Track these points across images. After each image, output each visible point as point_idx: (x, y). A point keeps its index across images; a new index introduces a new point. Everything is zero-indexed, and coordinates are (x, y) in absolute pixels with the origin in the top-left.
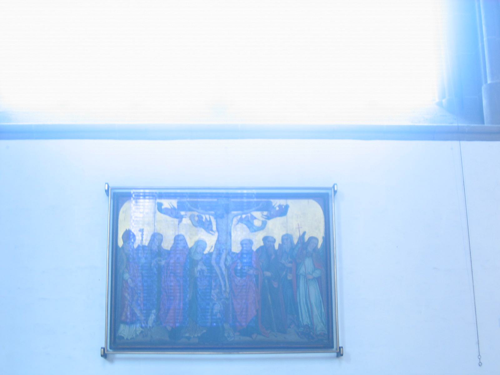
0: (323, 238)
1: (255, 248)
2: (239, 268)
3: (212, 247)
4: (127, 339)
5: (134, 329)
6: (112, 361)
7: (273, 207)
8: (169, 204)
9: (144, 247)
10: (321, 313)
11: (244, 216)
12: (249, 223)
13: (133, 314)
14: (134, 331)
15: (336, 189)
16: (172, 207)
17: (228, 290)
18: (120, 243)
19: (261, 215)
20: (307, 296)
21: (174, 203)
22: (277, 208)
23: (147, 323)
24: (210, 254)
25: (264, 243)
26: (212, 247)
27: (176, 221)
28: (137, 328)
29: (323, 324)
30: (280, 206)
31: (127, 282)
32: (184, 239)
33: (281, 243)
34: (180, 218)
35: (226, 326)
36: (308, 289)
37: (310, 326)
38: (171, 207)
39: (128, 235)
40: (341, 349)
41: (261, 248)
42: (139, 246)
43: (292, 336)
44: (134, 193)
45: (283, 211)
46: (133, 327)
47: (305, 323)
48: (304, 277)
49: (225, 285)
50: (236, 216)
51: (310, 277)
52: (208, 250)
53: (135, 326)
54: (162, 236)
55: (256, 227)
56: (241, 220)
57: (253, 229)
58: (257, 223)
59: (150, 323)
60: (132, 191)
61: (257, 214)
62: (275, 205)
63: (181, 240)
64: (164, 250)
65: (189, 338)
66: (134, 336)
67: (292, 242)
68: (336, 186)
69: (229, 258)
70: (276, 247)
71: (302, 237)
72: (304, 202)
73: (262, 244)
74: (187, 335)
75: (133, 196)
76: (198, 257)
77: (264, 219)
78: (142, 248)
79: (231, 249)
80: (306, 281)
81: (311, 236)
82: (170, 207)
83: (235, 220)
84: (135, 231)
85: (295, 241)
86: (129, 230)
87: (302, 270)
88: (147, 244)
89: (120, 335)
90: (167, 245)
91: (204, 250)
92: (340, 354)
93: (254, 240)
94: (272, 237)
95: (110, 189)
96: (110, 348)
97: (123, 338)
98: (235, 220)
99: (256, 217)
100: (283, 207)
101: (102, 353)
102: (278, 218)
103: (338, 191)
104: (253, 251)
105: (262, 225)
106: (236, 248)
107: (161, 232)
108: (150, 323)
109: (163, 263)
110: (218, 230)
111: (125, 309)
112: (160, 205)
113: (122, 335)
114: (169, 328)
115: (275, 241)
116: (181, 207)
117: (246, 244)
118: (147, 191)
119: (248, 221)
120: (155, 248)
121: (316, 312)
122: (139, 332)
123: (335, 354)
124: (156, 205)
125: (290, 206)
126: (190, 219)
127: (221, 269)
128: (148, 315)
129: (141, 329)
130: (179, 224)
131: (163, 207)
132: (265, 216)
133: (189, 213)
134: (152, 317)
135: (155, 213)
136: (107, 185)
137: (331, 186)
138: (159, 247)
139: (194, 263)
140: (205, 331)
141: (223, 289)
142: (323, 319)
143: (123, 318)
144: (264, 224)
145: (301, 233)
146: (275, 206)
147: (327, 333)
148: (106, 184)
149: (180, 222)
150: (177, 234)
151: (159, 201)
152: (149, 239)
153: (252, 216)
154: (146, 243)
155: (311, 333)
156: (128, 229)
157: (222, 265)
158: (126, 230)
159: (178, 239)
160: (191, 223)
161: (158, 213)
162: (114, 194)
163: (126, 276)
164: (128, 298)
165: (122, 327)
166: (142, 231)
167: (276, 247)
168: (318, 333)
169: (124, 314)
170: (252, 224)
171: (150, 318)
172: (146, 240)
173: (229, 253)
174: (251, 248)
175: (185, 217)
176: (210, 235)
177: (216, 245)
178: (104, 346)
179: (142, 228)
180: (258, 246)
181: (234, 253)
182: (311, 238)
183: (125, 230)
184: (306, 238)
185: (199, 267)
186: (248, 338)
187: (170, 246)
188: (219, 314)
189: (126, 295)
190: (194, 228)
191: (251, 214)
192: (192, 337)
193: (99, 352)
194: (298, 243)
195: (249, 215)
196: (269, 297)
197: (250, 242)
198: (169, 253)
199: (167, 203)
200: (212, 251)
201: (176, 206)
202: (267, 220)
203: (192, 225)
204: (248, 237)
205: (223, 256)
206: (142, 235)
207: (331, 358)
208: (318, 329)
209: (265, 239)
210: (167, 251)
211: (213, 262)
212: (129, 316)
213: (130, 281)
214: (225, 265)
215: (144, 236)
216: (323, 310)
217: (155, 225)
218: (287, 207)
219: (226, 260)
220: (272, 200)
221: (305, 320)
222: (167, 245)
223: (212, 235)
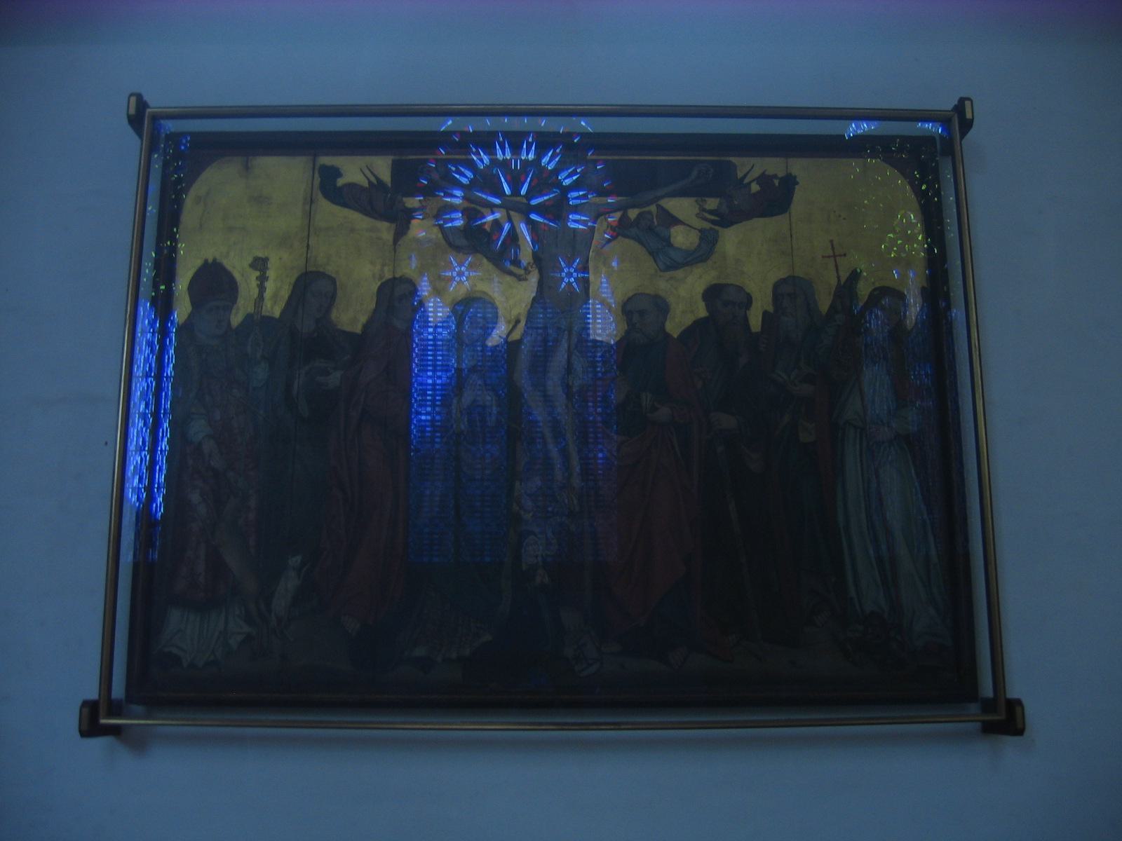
0: (923, 289)
1: (674, 327)
3: (518, 322)
8: (361, 170)
9: (268, 320)
11: (633, 214)
15: (969, 116)
16: (375, 182)
17: (576, 482)
19: (697, 210)
21: (382, 167)
22: (755, 188)
24: (511, 347)
25: (707, 306)
26: (518, 322)
27: (385, 230)
30: (764, 179)
32: (414, 291)
33: (771, 309)
34: (402, 220)
38: (370, 182)
40: (1018, 709)
41: (699, 325)
42: (249, 317)
54: (333, 281)
55: (679, 249)
56: (621, 229)
58: (682, 238)
61: (682, 207)
62: (745, 176)
64: (344, 332)
68: (967, 103)
69: (578, 364)
70: (755, 322)
71: (847, 288)
73: (702, 312)
74: (420, 652)
77: (707, 225)
78: (256, 322)
79: (585, 328)
82: (366, 184)
84: (238, 265)
85: (824, 304)
86: (215, 260)
88: (277, 313)
93: (671, 300)
94: (740, 289)
99: (681, 217)
100: (776, 182)
102: (758, 222)
103: (975, 123)
104: (667, 336)
105: (699, 245)
107: (330, 270)
109: (335, 379)
110: (537, 259)
112: (329, 175)
113: (175, 651)
115: (749, 300)
116: (406, 178)
117: (642, 313)
119: (650, 229)
123: (978, 725)
124: (317, 175)
125: (798, 180)
127: (546, 398)
130: (395, 241)
132: (711, 212)
134: (289, 584)
135: (312, 201)
136: (133, 100)
137: (948, 104)
140: (487, 638)
141: (559, 475)
145: (844, 275)
146: (746, 181)
149: (401, 231)
150: (388, 276)
151: (326, 160)
152: (285, 293)
153: (664, 213)
154: (274, 308)
156: (210, 261)
157: (554, 384)
158: (206, 261)
160: (440, 235)
165: (175, 615)
166: (260, 264)
167: (755, 322)
170: (667, 242)
172: (275, 296)
173: (584, 344)
176: (508, 278)
177: (530, 316)
178: (93, 693)
180: (688, 320)
182: (882, 292)
183: (199, 263)
184: (864, 290)
187: (363, 319)
189: (195, 497)
191: (660, 208)
193: (71, 720)
194: (832, 307)
195: (653, 208)
197: (661, 307)
198: (359, 342)
199: (353, 170)
200: (516, 335)
201: (386, 176)
203: (443, 242)
205: (560, 358)
209: (713, 294)
210: (349, 335)
211: (523, 378)
214: (567, 388)
215: (270, 286)
217: (308, 246)
218: (789, 183)
219: (569, 369)
220: (734, 160)
223: (520, 278)
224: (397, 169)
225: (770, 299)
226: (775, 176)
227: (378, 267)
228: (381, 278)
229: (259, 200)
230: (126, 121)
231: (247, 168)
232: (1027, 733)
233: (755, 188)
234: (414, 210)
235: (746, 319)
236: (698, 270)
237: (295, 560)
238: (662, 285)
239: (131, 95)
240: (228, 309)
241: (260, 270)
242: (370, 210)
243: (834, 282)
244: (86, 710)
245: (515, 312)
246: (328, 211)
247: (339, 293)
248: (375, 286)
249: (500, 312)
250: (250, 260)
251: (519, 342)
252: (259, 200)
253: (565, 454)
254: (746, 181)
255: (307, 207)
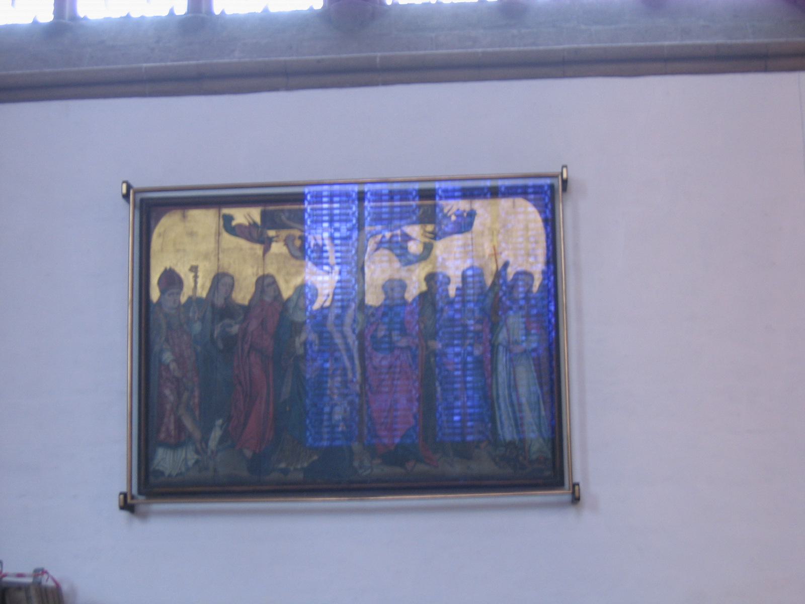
2: (381, 333)
4: (170, 476)
5: (184, 456)
6: (144, 516)
7: (446, 217)
8: (245, 217)
9: (199, 301)
10: (539, 416)
12: (398, 247)
13: (180, 427)
14: (183, 460)
15: (565, 176)
16: (251, 221)
18: (155, 294)
19: (422, 232)
20: (513, 386)
21: (255, 214)
22: (453, 218)
23: (207, 444)
27: (258, 249)
28: (188, 455)
29: (544, 439)
31: (167, 367)
34: (267, 243)
35: (356, 446)
36: (514, 371)
37: (517, 443)
38: (250, 224)
39: (171, 280)
40: (577, 488)
41: (422, 296)
42: (190, 298)
43: (484, 466)
44: (309, 193)
45: (465, 223)
46: (181, 454)
47: (508, 438)
48: (505, 349)
49: (353, 369)
50: (373, 235)
51: (518, 349)
52: (321, 303)
53: (184, 451)
54: (232, 278)
56: (380, 245)
57: (406, 259)
58: (414, 248)
59: (213, 444)
60: (306, 190)
61: (414, 231)
62: (448, 211)
63: (269, 285)
65: (285, 471)
66: (183, 469)
67: (482, 283)
68: (565, 170)
69: (360, 318)
72: (505, 203)
73: (424, 288)
74: (283, 465)
75: (309, 197)
76: (299, 317)
77: (427, 240)
79: (362, 301)
80: (511, 360)
81: (519, 269)
83: (371, 245)
84: (183, 271)
85: (489, 281)
87: (502, 336)
89: (157, 468)
90: (243, 295)
91: (312, 302)
92: (576, 499)
93: (408, 282)
95: (131, 192)
96: (140, 492)
97: (162, 473)
98: (371, 245)
101: (122, 504)
102: (456, 236)
106: (374, 298)
107: (231, 271)
108: (213, 444)
109: (235, 329)
111: (166, 420)
112: (228, 219)
113: (161, 469)
114: (248, 453)
115: (448, 281)
116: (269, 220)
118: (336, 188)
120: (219, 301)
121: (529, 417)
122: (193, 461)
123: (568, 497)
126: (286, 244)
127: (344, 337)
128: (207, 431)
129: (196, 457)
131: (234, 223)
132: (430, 233)
133: (284, 233)
134: (216, 434)
136: (124, 186)
138: (228, 298)
139: (297, 328)
140: (315, 458)
141: (350, 375)
142: (543, 430)
143: (162, 436)
144: (428, 249)
145: (500, 264)
146: (449, 214)
147: (550, 456)
148: (124, 182)
149: (266, 250)
150: (261, 273)
151: (226, 211)
154: (203, 293)
155: (521, 458)
156: (168, 268)
159: (265, 283)
161: (226, 236)
162: (142, 200)
163: (168, 357)
164: (172, 398)
166: (194, 269)
167: (452, 292)
168: (534, 457)
169: (163, 429)
170: (405, 249)
171: (213, 435)
172: (203, 286)
173: (362, 305)
174: (403, 298)
175: (276, 241)
178: (124, 489)
179: (194, 263)
181: (371, 307)
183: (161, 270)
184: (511, 272)
185: (303, 337)
186: (398, 470)
187: (249, 297)
188: (341, 424)
189: (167, 392)
190: (293, 261)
191: (402, 231)
192: (292, 468)
193: (115, 502)
195: (398, 232)
196: (439, 389)
197: (403, 286)
198: (247, 310)
199: (241, 216)
200: (327, 304)
201: (258, 219)
202: (432, 241)
204: (397, 276)
206: (196, 277)
207: (560, 505)
208: (534, 448)
209: (431, 278)
210: (242, 307)
212: (173, 433)
213: (173, 366)
215: (200, 281)
216: (543, 413)
217: (218, 259)
218: (472, 214)
219: (354, 321)
221: (507, 433)
222: (243, 295)
224: (264, 215)
225: (459, 279)
226: (464, 211)
227: (255, 269)
228: (257, 274)
229: (191, 234)
230: (121, 197)
231: (184, 217)
232: (581, 498)
233: (453, 218)
234: (273, 237)
235: (447, 291)
236: (423, 264)
237: (219, 422)
238: (403, 274)
239: (124, 182)
240: (179, 294)
241: (194, 272)
242: (250, 238)
243: (494, 268)
244: (122, 496)
245: (326, 292)
246: (228, 240)
247: (236, 284)
248: (254, 280)
249: (319, 291)
250: (189, 267)
251: (328, 308)
252: (191, 234)
253: (353, 364)
254: (449, 214)
255: (217, 237)
